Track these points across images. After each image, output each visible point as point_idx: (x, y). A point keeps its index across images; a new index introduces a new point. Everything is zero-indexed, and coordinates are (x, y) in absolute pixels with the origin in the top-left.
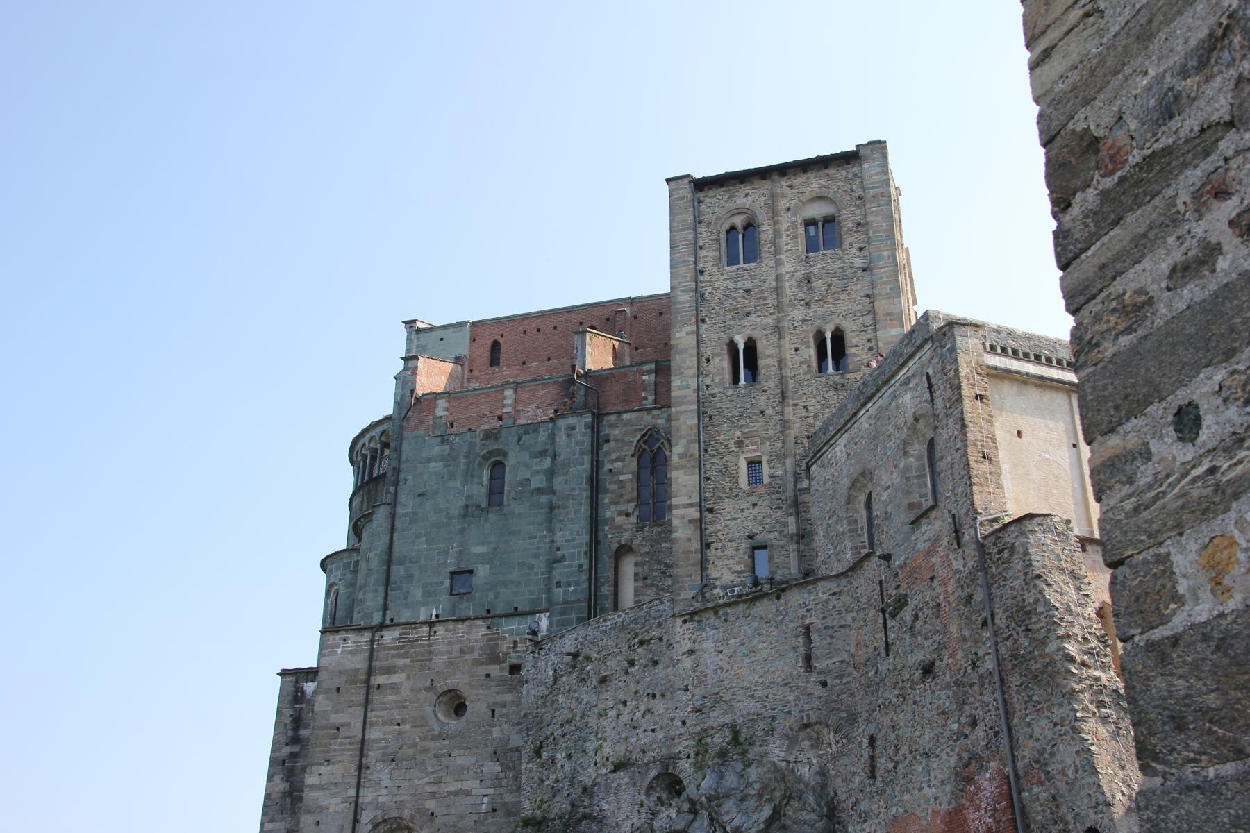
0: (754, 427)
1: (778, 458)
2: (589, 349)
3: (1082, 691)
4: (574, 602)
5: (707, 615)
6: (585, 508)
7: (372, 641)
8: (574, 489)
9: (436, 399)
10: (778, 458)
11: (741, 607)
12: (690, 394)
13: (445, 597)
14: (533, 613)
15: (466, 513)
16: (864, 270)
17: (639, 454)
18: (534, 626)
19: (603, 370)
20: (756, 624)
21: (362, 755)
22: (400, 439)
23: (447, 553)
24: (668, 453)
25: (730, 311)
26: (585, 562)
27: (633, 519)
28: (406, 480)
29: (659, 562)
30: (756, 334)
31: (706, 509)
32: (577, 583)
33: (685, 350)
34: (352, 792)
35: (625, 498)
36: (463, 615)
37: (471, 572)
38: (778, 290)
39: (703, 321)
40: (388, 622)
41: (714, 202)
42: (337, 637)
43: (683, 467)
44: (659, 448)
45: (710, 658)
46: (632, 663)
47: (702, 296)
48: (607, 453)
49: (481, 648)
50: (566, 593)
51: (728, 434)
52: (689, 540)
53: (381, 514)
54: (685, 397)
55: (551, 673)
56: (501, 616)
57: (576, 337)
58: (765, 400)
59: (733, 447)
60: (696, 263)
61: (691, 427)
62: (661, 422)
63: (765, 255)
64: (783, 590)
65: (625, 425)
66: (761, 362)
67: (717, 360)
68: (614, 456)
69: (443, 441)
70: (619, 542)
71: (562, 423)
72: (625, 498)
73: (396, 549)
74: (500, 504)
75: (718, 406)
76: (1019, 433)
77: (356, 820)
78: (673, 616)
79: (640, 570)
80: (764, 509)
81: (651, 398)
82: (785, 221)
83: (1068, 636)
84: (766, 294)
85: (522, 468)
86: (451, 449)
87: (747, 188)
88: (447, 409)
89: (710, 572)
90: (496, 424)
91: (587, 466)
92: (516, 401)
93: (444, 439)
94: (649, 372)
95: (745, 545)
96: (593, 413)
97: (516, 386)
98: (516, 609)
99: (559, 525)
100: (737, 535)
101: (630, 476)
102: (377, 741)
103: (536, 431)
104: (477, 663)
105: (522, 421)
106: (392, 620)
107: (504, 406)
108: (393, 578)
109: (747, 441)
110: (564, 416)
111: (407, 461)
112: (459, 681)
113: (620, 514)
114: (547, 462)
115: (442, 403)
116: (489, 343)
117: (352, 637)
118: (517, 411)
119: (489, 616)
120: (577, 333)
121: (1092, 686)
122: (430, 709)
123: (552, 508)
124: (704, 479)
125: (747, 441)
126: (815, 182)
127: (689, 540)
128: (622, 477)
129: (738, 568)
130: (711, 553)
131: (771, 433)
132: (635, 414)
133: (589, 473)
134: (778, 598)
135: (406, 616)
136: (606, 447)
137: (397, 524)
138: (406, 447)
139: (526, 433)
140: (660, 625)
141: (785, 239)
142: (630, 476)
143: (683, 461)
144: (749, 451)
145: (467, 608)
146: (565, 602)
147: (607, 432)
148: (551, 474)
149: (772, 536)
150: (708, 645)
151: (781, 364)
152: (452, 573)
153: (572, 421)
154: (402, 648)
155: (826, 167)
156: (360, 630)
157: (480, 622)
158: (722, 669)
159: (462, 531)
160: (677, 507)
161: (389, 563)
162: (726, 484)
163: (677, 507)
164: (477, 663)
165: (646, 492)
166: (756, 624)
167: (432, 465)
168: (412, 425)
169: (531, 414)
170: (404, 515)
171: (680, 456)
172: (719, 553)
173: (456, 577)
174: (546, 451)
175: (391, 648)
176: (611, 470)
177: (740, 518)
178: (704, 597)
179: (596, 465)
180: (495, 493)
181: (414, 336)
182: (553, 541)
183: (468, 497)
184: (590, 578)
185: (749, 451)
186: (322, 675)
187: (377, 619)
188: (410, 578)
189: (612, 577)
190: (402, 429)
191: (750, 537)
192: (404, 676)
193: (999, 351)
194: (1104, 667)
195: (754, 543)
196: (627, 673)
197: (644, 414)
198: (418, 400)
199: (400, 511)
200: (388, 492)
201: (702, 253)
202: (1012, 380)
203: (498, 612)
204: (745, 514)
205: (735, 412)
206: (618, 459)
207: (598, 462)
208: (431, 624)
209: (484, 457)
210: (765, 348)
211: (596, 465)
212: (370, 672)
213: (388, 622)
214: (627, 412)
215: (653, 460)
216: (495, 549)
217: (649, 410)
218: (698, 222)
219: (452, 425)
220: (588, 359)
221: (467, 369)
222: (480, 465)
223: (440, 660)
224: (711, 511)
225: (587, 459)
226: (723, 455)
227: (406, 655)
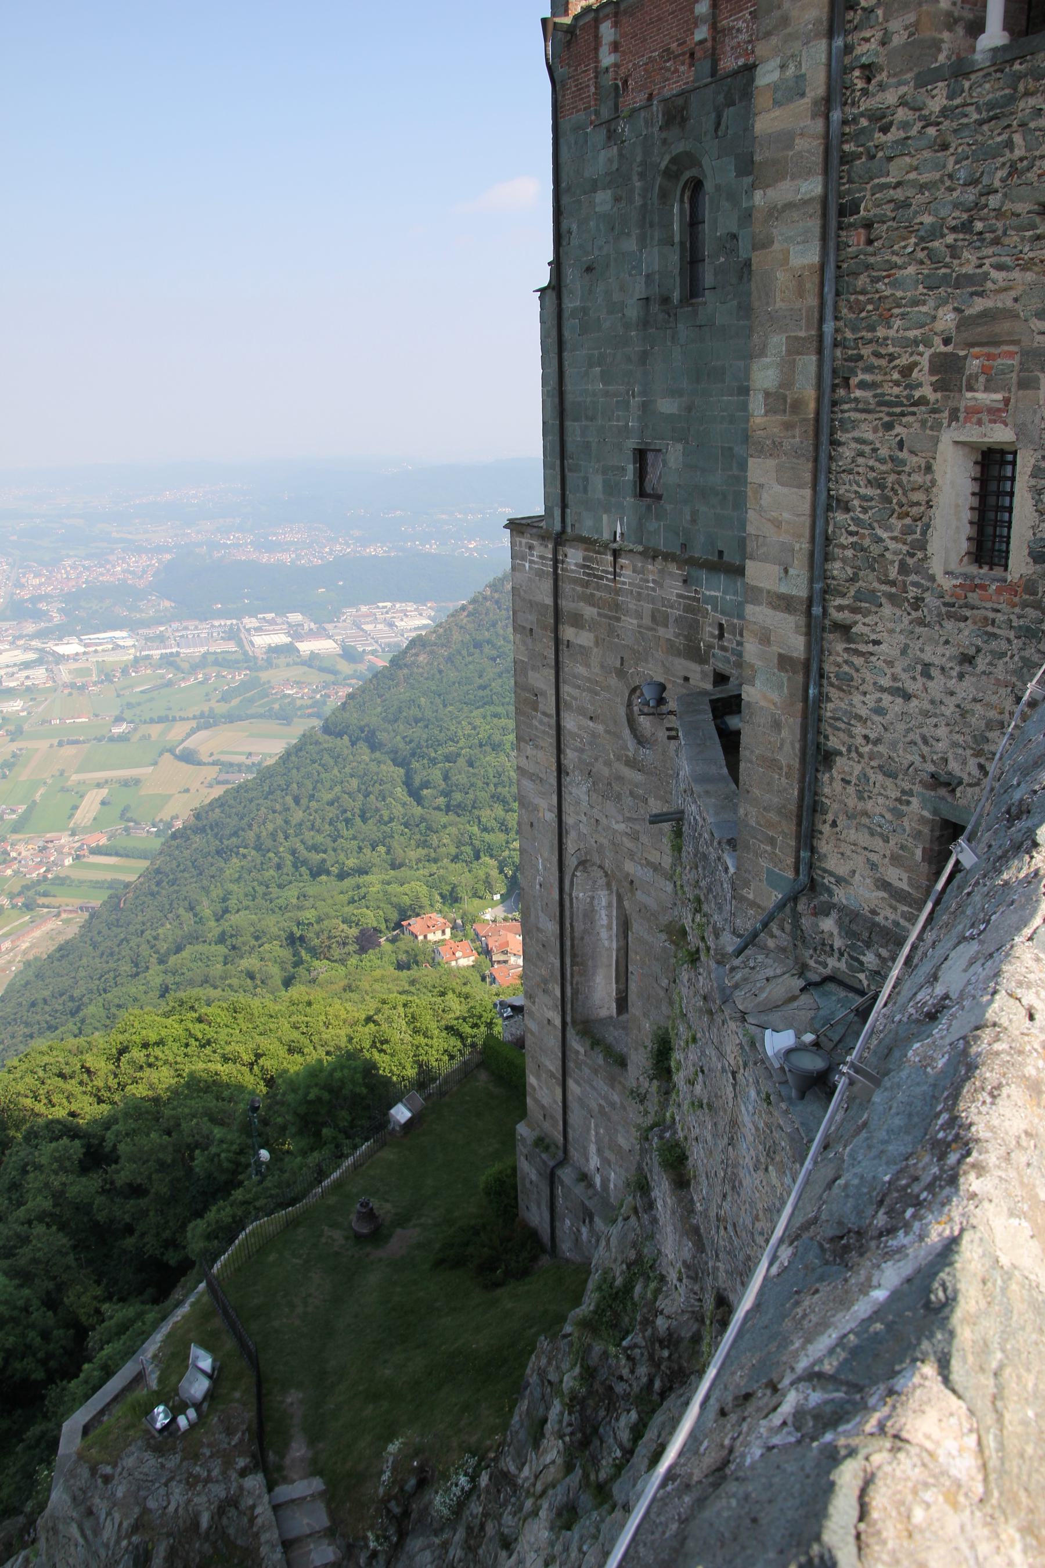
9: (597, 22)
13: (629, 500)
31: (818, 627)
86: (621, 155)
88: (615, 47)
98: (721, 553)
107: (696, 22)
108: (570, 447)
115: (607, 31)
159: (644, 357)
209: (667, 173)
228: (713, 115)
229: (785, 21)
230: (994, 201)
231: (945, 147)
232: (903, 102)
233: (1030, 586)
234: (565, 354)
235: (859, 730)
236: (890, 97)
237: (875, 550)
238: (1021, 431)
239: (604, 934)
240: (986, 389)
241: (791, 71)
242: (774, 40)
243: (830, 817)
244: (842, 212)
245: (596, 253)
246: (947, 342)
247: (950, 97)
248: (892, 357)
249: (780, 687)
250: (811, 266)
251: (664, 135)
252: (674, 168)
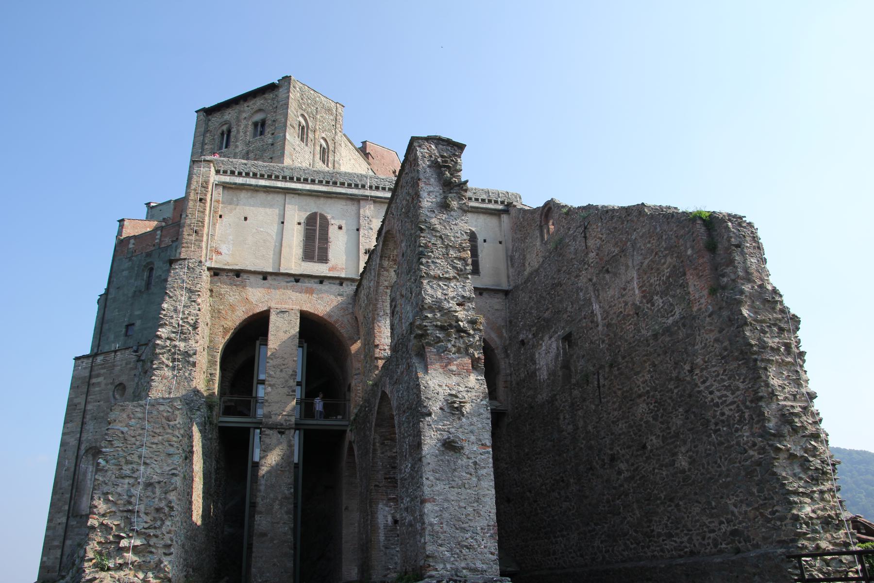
3: (163, 354)
13: (122, 338)
16: (272, 145)
21: (84, 417)
34: (78, 435)
37: (133, 324)
41: (216, 119)
63: (231, 144)
73: (106, 316)
76: (246, 219)
77: (79, 448)
82: (244, 122)
83: (166, 324)
87: (230, 111)
90: (152, 248)
93: (130, 259)
102: (90, 410)
105: (163, 246)
112: (123, 379)
115: (132, 241)
117: (85, 360)
118: (161, 241)
121: (170, 350)
122: (111, 393)
126: (258, 102)
137: (108, 304)
141: (241, 134)
145: (131, 342)
152: (127, 326)
155: (264, 93)
180: (148, 284)
187: (95, 351)
193: (244, 174)
194: (185, 340)
198: (122, 241)
199: (110, 297)
201: (206, 147)
202: (247, 190)
208: (115, 351)
212: (90, 377)
218: (207, 131)
222: (143, 270)
239: (89, 482)
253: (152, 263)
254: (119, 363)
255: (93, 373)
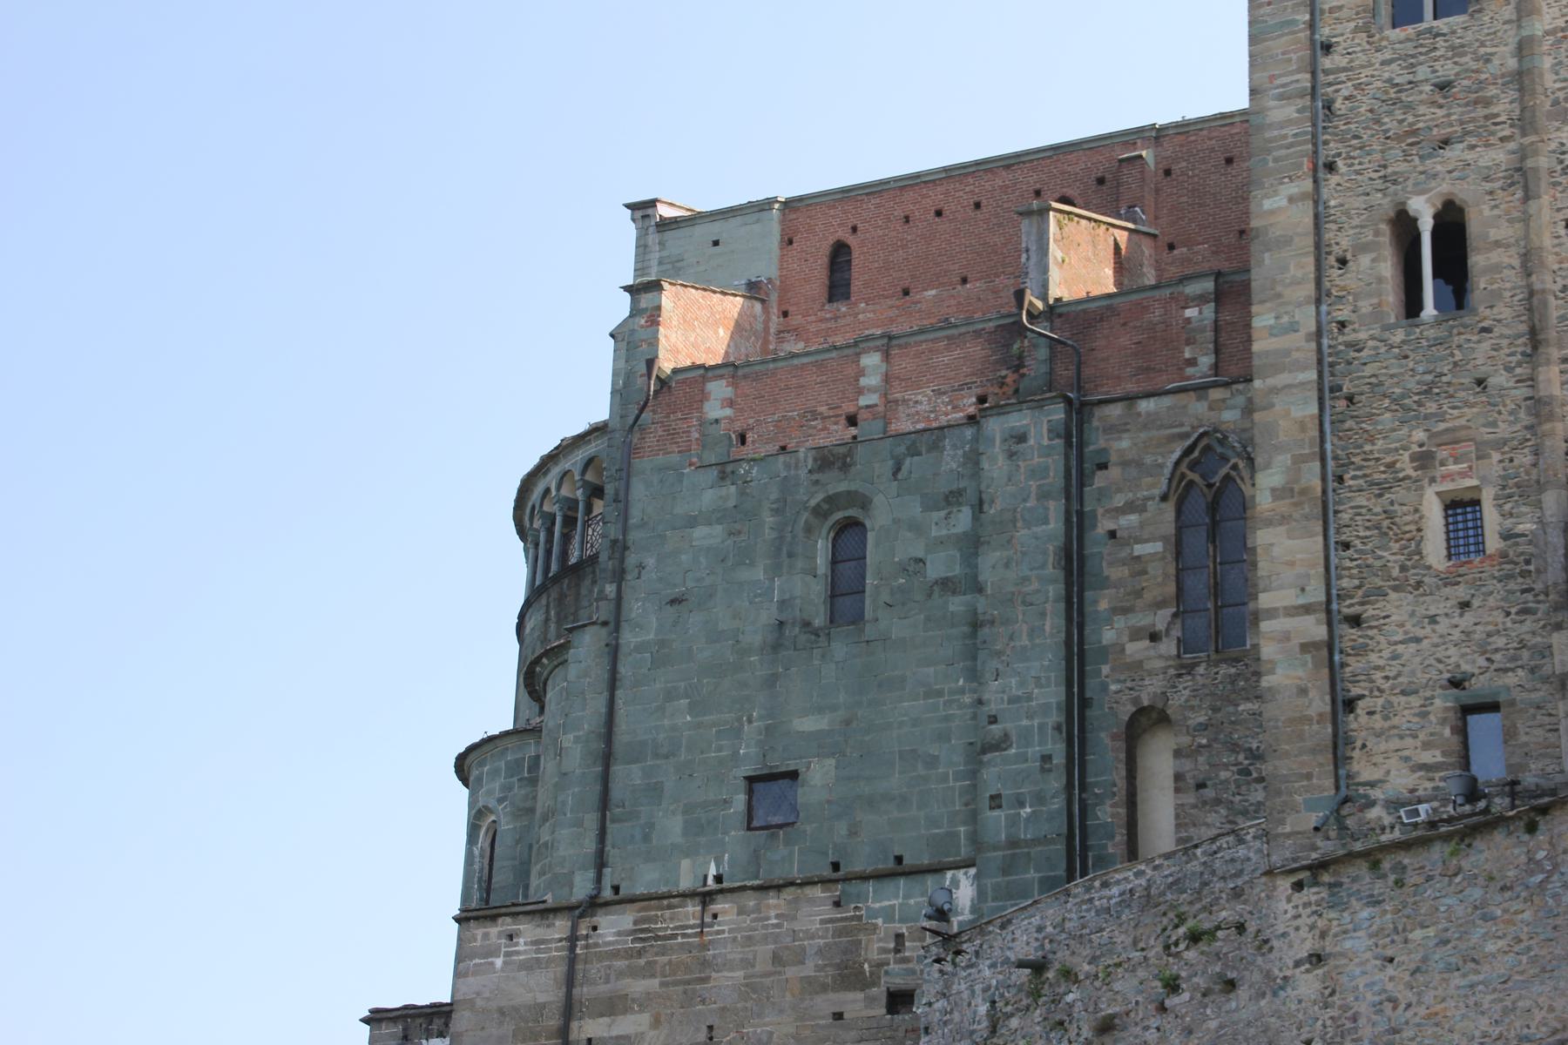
0: (1457, 418)
1: (1523, 490)
2: (1055, 251)
4: (1036, 841)
5: (1352, 871)
6: (1053, 624)
7: (573, 939)
8: (1026, 579)
10: (1523, 490)
11: (1438, 852)
12: (1300, 345)
14: (938, 870)
15: (779, 639)
17: (1180, 493)
18: (940, 899)
19: (1090, 299)
20: (1476, 893)
22: (626, 473)
23: (737, 733)
24: (1246, 489)
25: (1399, 138)
26: (1058, 750)
27: (1168, 647)
28: (641, 567)
29: (1234, 748)
30: (1465, 192)
31: (1342, 617)
32: (1039, 799)
33: (1286, 241)
35: (1148, 596)
36: (778, 875)
37: (793, 775)
38: (1522, 79)
39: (1331, 167)
40: (607, 894)
42: (494, 931)
43: (1284, 519)
44: (1227, 477)
45: (1363, 975)
46: (1173, 986)
47: (1328, 106)
48: (1102, 494)
49: (820, 952)
50: (1013, 821)
51: (1394, 438)
52: (1303, 691)
53: (587, 648)
54: (1287, 353)
55: (983, 1009)
56: (864, 878)
57: (1025, 224)
58: (1488, 347)
59: (1407, 467)
60: (1312, 26)
61: (1302, 426)
62: (1230, 416)
64: (1544, 811)
65: (1145, 427)
66: (1477, 260)
67: (1365, 260)
68: (1119, 500)
69: (723, 476)
70: (1136, 701)
71: (994, 427)
72: (1148, 596)
74: (858, 619)
75: (1368, 370)
78: (1269, 873)
79: (1187, 765)
80: (1488, 616)
81: (1206, 361)
84: (1492, 91)
85: (903, 533)
86: (742, 493)
88: (731, 403)
89: (1355, 767)
90: (843, 433)
91: (1055, 525)
92: (887, 378)
93: (725, 471)
94: (1201, 300)
95: (1443, 703)
96: (1069, 402)
97: (888, 344)
98: (899, 859)
99: (994, 664)
100: (1422, 678)
101: (1156, 547)
103: (936, 447)
104: (813, 986)
105: (905, 425)
106: (616, 889)
107: (861, 391)
108: (616, 793)
109: (1443, 453)
110: (1000, 410)
111: (643, 525)
113: (1135, 635)
114: (963, 519)
115: (719, 389)
116: (825, 249)
117: (528, 931)
119: (837, 876)
120: (1028, 213)
123: (975, 625)
124: (1336, 545)
125: (1443, 453)
127: (1303, 691)
128: (1139, 549)
129: (1428, 757)
130: (1358, 723)
131: (1503, 430)
132: (1167, 401)
133: (1061, 541)
134: (1532, 828)
135: (646, 879)
136: (1100, 480)
137: (624, 670)
138: (638, 490)
139: (914, 451)
140: (1237, 894)
142: (1156, 547)
143: (1283, 506)
144: (1449, 477)
145: (787, 859)
146: (1013, 843)
147: (1102, 443)
148: (972, 544)
149: (1510, 679)
150: (1358, 943)
151: (1529, 261)
152: (751, 780)
153: (1019, 420)
154: (640, 953)
156: (545, 913)
157: (817, 892)
158: (1394, 1001)
159: (771, 681)
160: (1272, 613)
161: (607, 758)
162: (1392, 557)
163: (1272, 613)
164: (813, 986)
165: (1198, 584)
166: (1476, 893)
167: (699, 532)
168: (651, 440)
169: (926, 406)
170: (640, 648)
171: (1277, 494)
172: (1378, 722)
173: (758, 786)
174: (959, 493)
175: (615, 955)
176: (1112, 534)
177: (1423, 639)
178: (1343, 828)
179: (1077, 522)
180: (845, 592)
181: (653, 238)
182: (980, 702)
183: (783, 603)
184: (1069, 785)
185: (1449, 477)
186: (460, 1021)
187: (582, 888)
188: (655, 791)
189: (1122, 784)
190: (630, 451)
191: (1456, 683)
192: (645, 1018)
195: (1466, 697)
196: (1162, 1008)
197: (1189, 399)
198: (663, 383)
199: (629, 638)
200: (602, 597)
203: (858, 868)
204: (1443, 626)
205: (1412, 384)
206: (1130, 508)
207: (1080, 514)
208: (706, 898)
210: (1488, 226)
211: (1077, 522)
212: (569, 1010)
213: (607, 894)
214: (1148, 395)
215: (1213, 507)
216: (848, 722)
217: (1201, 389)
219: (743, 439)
220: (1055, 274)
221: (775, 310)
222: (808, 530)
223: (726, 981)
224: (1355, 621)
225: (1055, 508)
226: (1382, 489)
227: (649, 971)
228: (891, 463)
229: (1279, 296)
230: (1444, 379)
231: (1406, 357)
232: (1372, 338)
233: (1503, 555)
234: (619, 693)
235: (1378, 675)
236: (1363, 336)
237: (1378, 563)
238: (1483, 479)
240: (1455, 463)
241: (1285, 319)
242: (1268, 305)
243: (1359, 744)
244: (1332, 390)
245: (690, 584)
246: (1421, 445)
247: (1407, 335)
248: (1378, 459)
249: (1304, 664)
250: (1312, 417)
251: (815, 477)
252: (826, 507)
253: (864, 503)
254: (734, 953)
255: (582, 992)
